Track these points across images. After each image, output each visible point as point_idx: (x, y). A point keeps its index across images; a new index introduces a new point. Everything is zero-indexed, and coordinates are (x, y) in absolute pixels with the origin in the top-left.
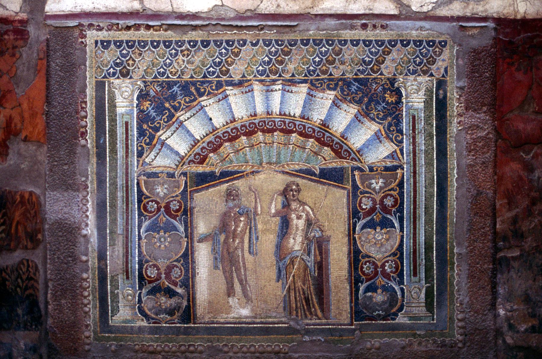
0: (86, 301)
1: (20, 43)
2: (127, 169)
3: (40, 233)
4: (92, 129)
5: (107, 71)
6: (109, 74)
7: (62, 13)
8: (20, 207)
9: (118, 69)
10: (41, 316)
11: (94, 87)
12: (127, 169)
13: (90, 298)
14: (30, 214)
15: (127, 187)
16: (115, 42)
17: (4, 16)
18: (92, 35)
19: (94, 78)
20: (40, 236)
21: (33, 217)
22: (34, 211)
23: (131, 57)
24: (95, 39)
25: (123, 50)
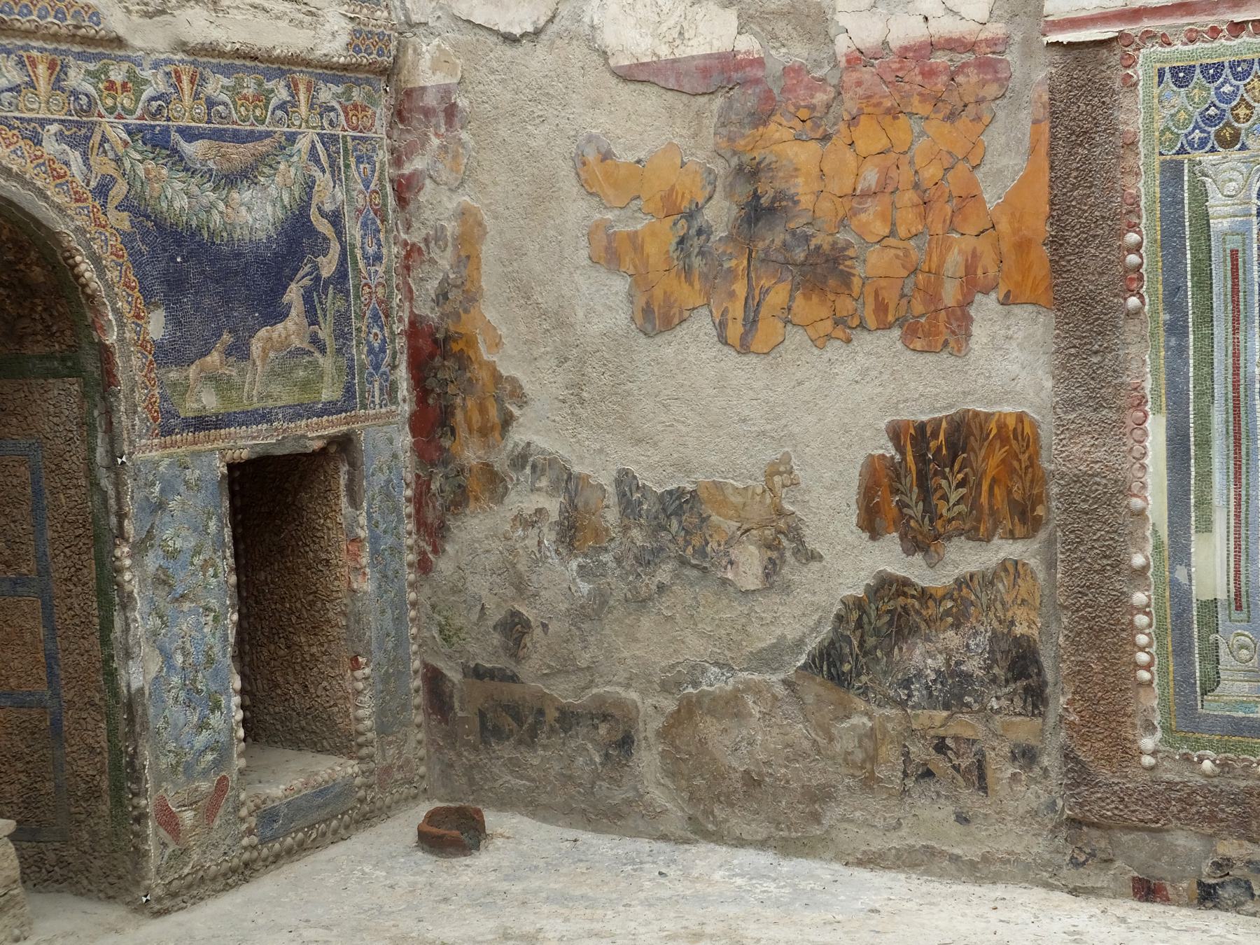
0: (1143, 657)
1: (992, 90)
2: (1236, 356)
3: (1041, 502)
4: (1152, 271)
5: (1186, 136)
6: (1191, 144)
7: (1083, 14)
8: (998, 446)
9: (1213, 130)
10: (1045, 683)
11: (1158, 176)
12: (1236, 356)
13: (1153, 650)
14: (1019, 461)
15: (1236, 399)
16: (1205, 68)
17: (955, 35)
18: (1149, 57)
19: (1157, 156)
20: (1040, 510)
21: (1027, 468)
22: (1027, 455)
23: (1243, 99)
24: (1159, 65)
25: (1223, 84)
